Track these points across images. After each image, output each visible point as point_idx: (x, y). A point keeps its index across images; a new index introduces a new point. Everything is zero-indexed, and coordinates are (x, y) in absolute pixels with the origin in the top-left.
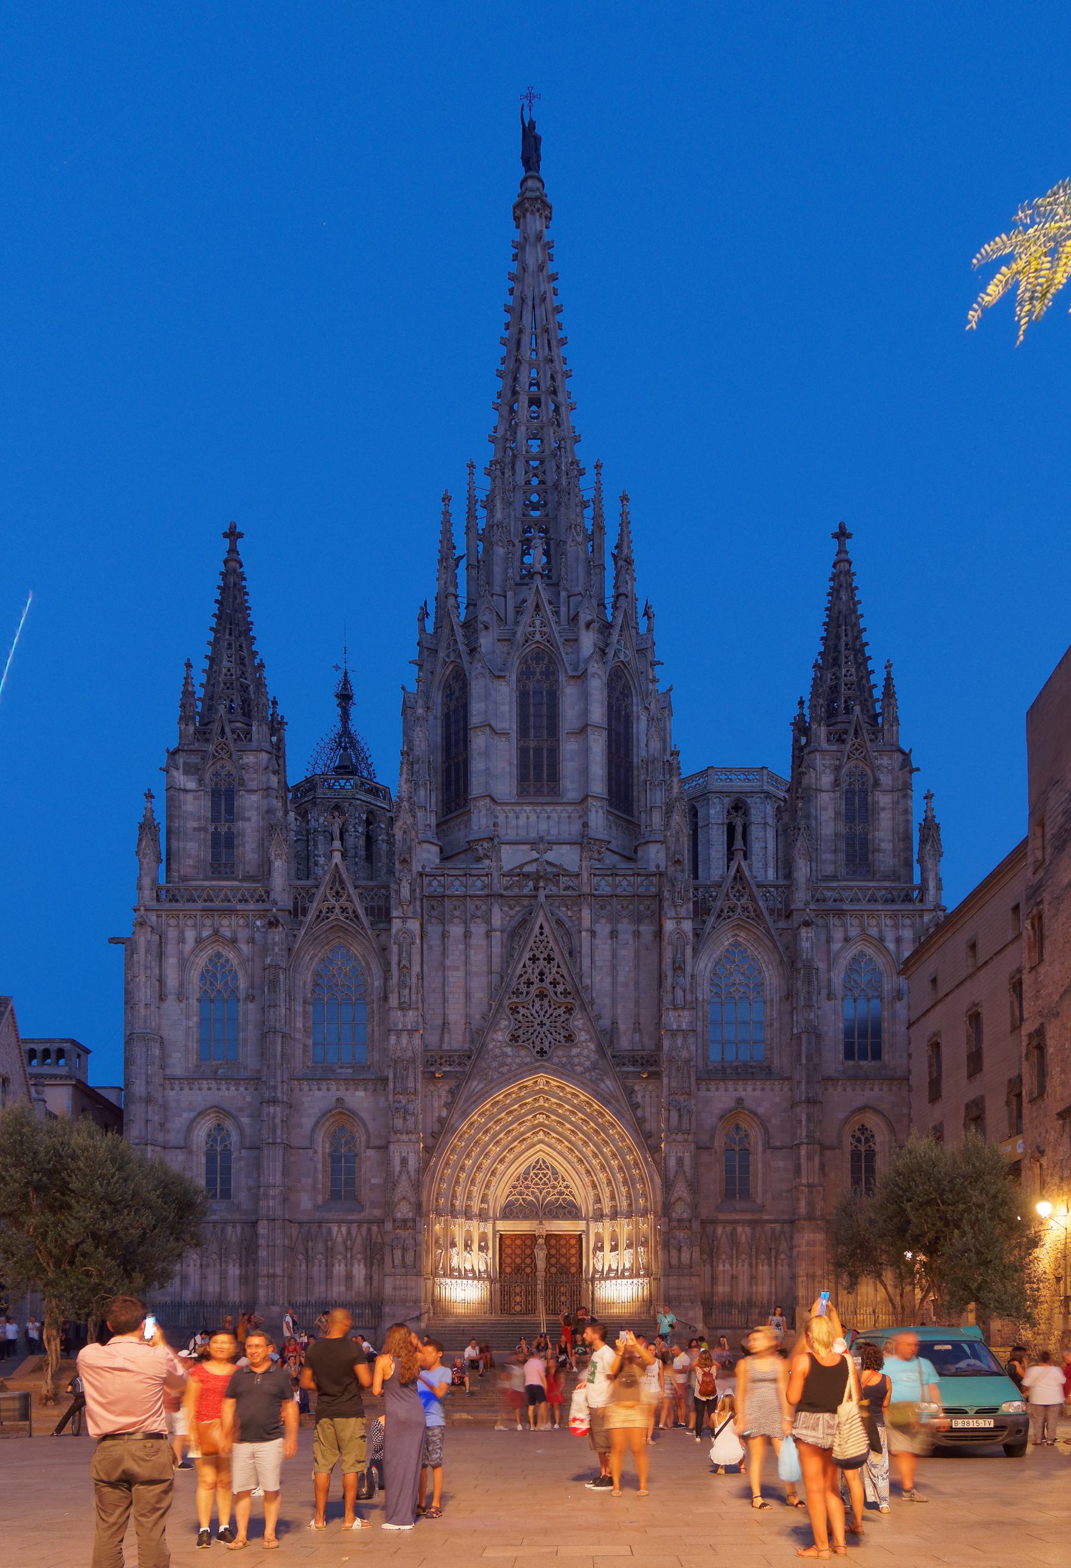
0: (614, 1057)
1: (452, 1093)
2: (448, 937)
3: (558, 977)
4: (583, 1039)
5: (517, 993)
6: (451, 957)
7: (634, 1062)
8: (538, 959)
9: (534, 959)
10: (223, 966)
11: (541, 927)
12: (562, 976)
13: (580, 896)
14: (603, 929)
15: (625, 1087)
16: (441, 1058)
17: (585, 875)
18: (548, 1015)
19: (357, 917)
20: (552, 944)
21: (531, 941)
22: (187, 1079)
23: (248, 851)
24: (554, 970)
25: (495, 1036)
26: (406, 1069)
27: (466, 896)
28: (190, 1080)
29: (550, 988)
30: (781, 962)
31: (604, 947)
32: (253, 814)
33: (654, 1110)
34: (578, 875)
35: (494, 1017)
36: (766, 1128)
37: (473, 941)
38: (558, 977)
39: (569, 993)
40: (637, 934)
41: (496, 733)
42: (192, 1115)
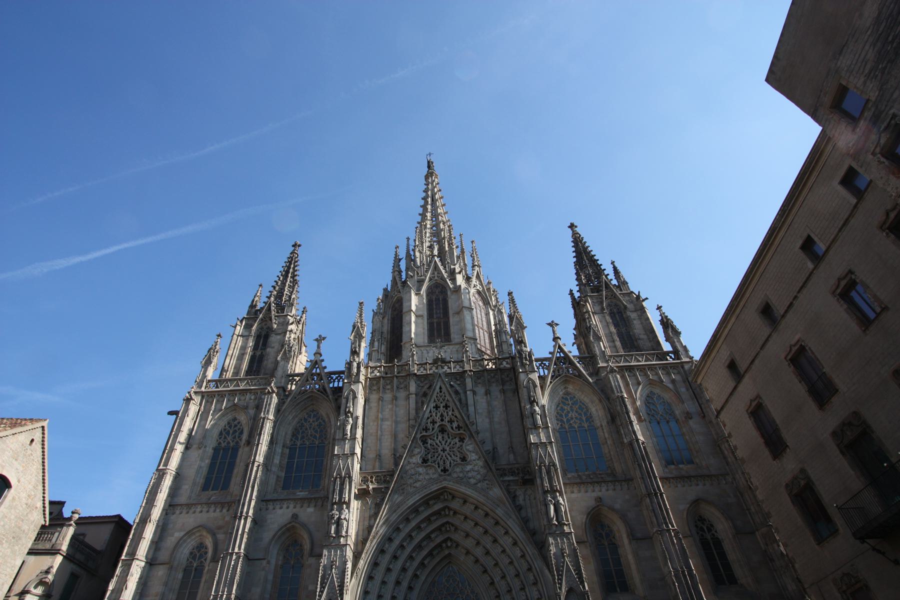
3: (453, 418)
4: (473, 458)
5: (426, 429)
7: (513, 473)
9: (437, 407)
10: (236, 426)
11: (440, 388)
14: (481, 390)
15: (509, 492)
16: (372, 477)
19: (325, 390)
20: (448, 397)
21: (434, 396)
22: (187, 505)
23: (268, 363)
24: (450, 413)
25: (411, 460)
26: (342, 484)
27: (393, 377)
28: (189, 506)
29: (448, 425)
30: (600, 401)
31: (482, 401)
32: (277, 346)
36: (623, 517)
38: (453, 418)
40: (503, 392)
42: (182, 534)
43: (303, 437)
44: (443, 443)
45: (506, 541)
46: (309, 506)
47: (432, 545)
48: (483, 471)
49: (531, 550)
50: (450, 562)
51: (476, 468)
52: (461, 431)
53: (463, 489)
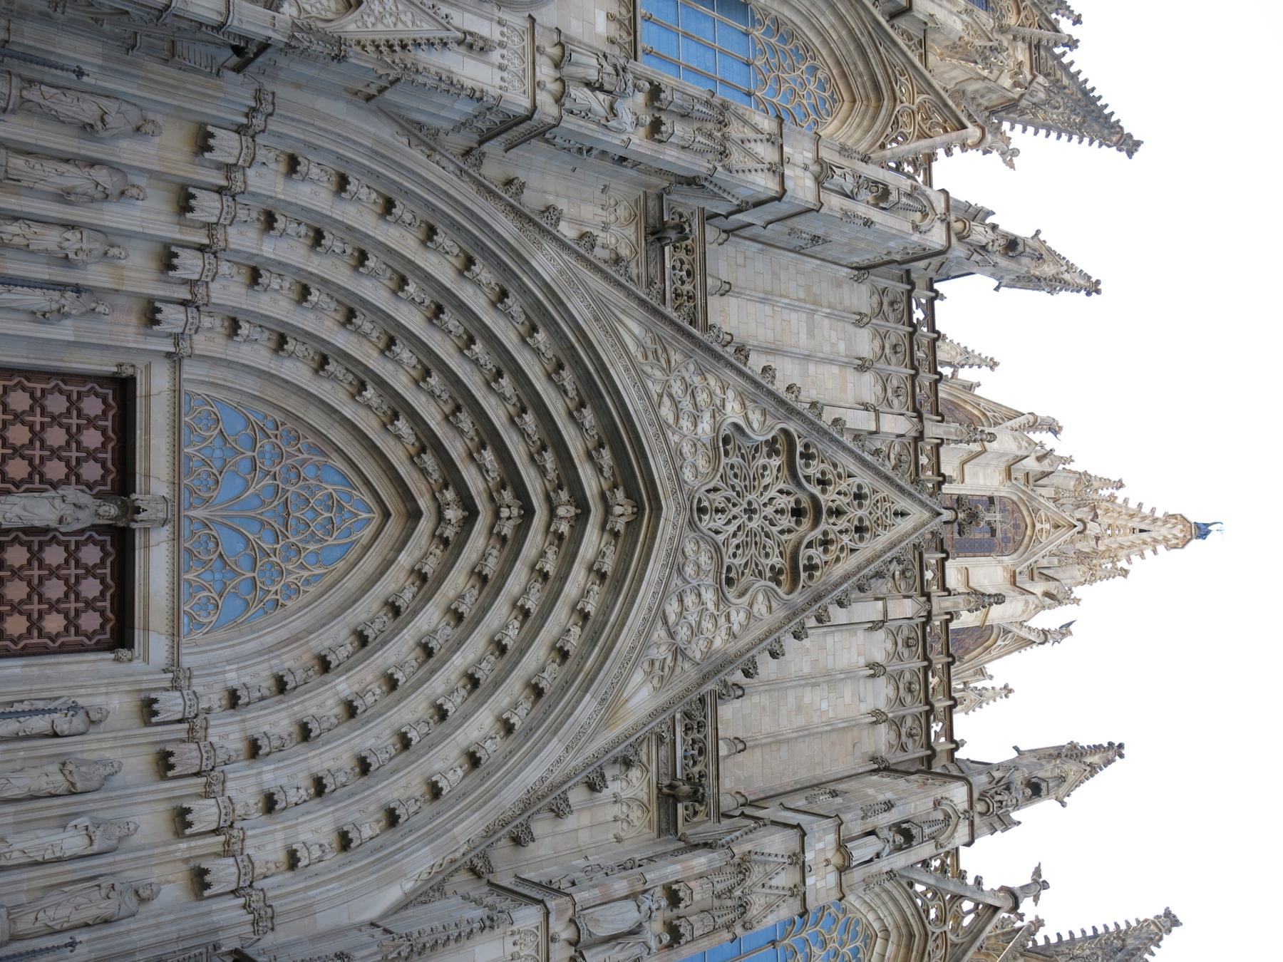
0: (702, 700)
1: (617, 260)
2: (859, 324)
6: (826, 321)
8: (860, 506)
9: (859, 496)
11: (903, 514)
12: (838, 559)
13: (928, 596)
14: (878, 647)
17: (948, 603)
18: (768, 528)
20: (885, 538)
21: (886, 491)
24: (845, 539)
25: (730, 394)
29: (817, 534)
33: (584, 837)
34: (945, 589)
35: (771, 394)
37: (851, 374)
39: (811, 577)
41: (964, 463)
43: (774, 52)
44: (769, 511)
45: (478, 727)
46: (610, 17)
47: (456, 449)
48: (696, 651)
49: (467, 828)
50: (386, 515)
51: (707, 624)
52: (803, 575)
53: (654, 571)
